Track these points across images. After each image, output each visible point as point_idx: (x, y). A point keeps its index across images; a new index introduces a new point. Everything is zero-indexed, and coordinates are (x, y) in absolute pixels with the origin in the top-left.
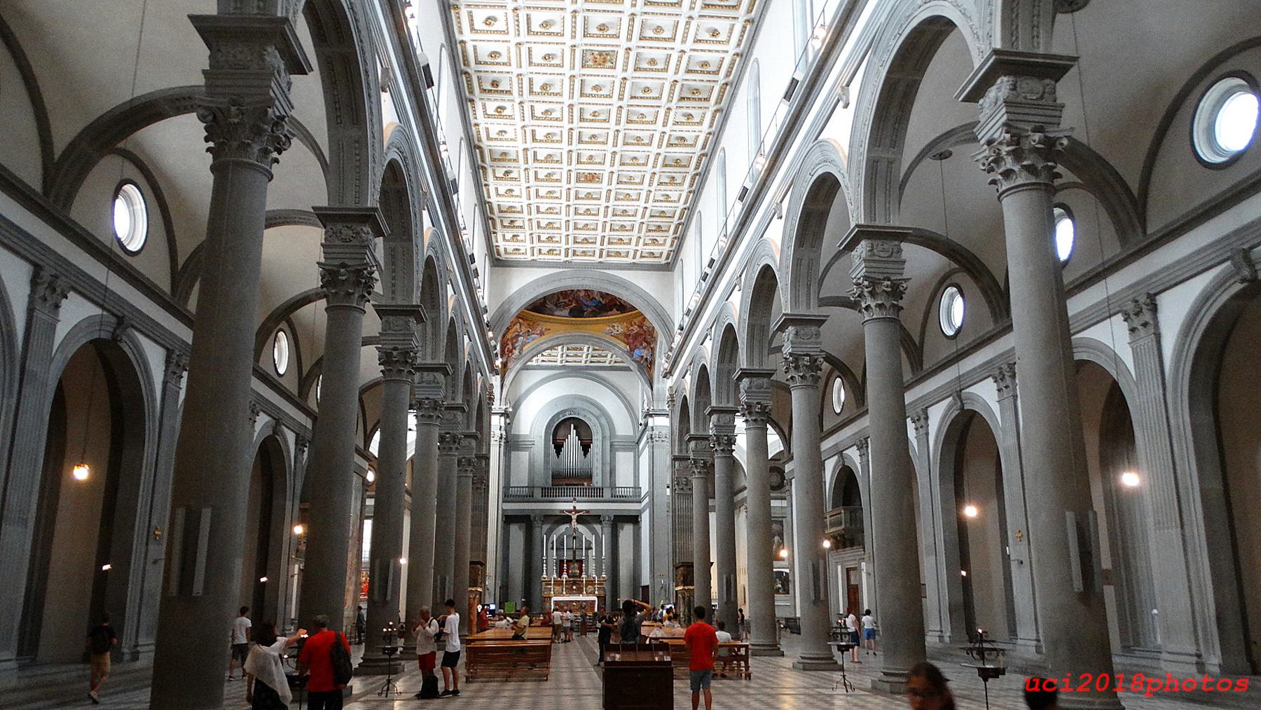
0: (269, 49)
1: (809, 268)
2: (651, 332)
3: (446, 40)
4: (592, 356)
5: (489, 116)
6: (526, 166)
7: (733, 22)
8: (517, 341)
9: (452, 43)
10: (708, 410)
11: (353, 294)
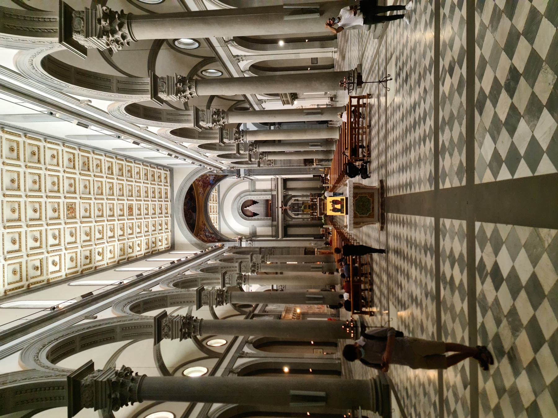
0: (83, 383)
1: (171, 114)
2: (202, 176)
3: (65, 283)
4: (214, 201)
5: (103, 258)
6: (126, 239)
7: (46, 148)
9: (67, 280)
10: (238, 154)
11: (194, 325)
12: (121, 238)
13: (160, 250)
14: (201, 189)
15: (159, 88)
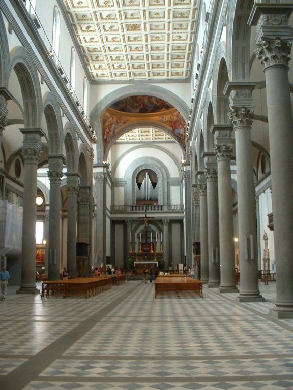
6: (97, 22)
8: (111, 127)
12: (98, 14)
13: (88, 66)
14: (167, 119)
15: (273, 15)
